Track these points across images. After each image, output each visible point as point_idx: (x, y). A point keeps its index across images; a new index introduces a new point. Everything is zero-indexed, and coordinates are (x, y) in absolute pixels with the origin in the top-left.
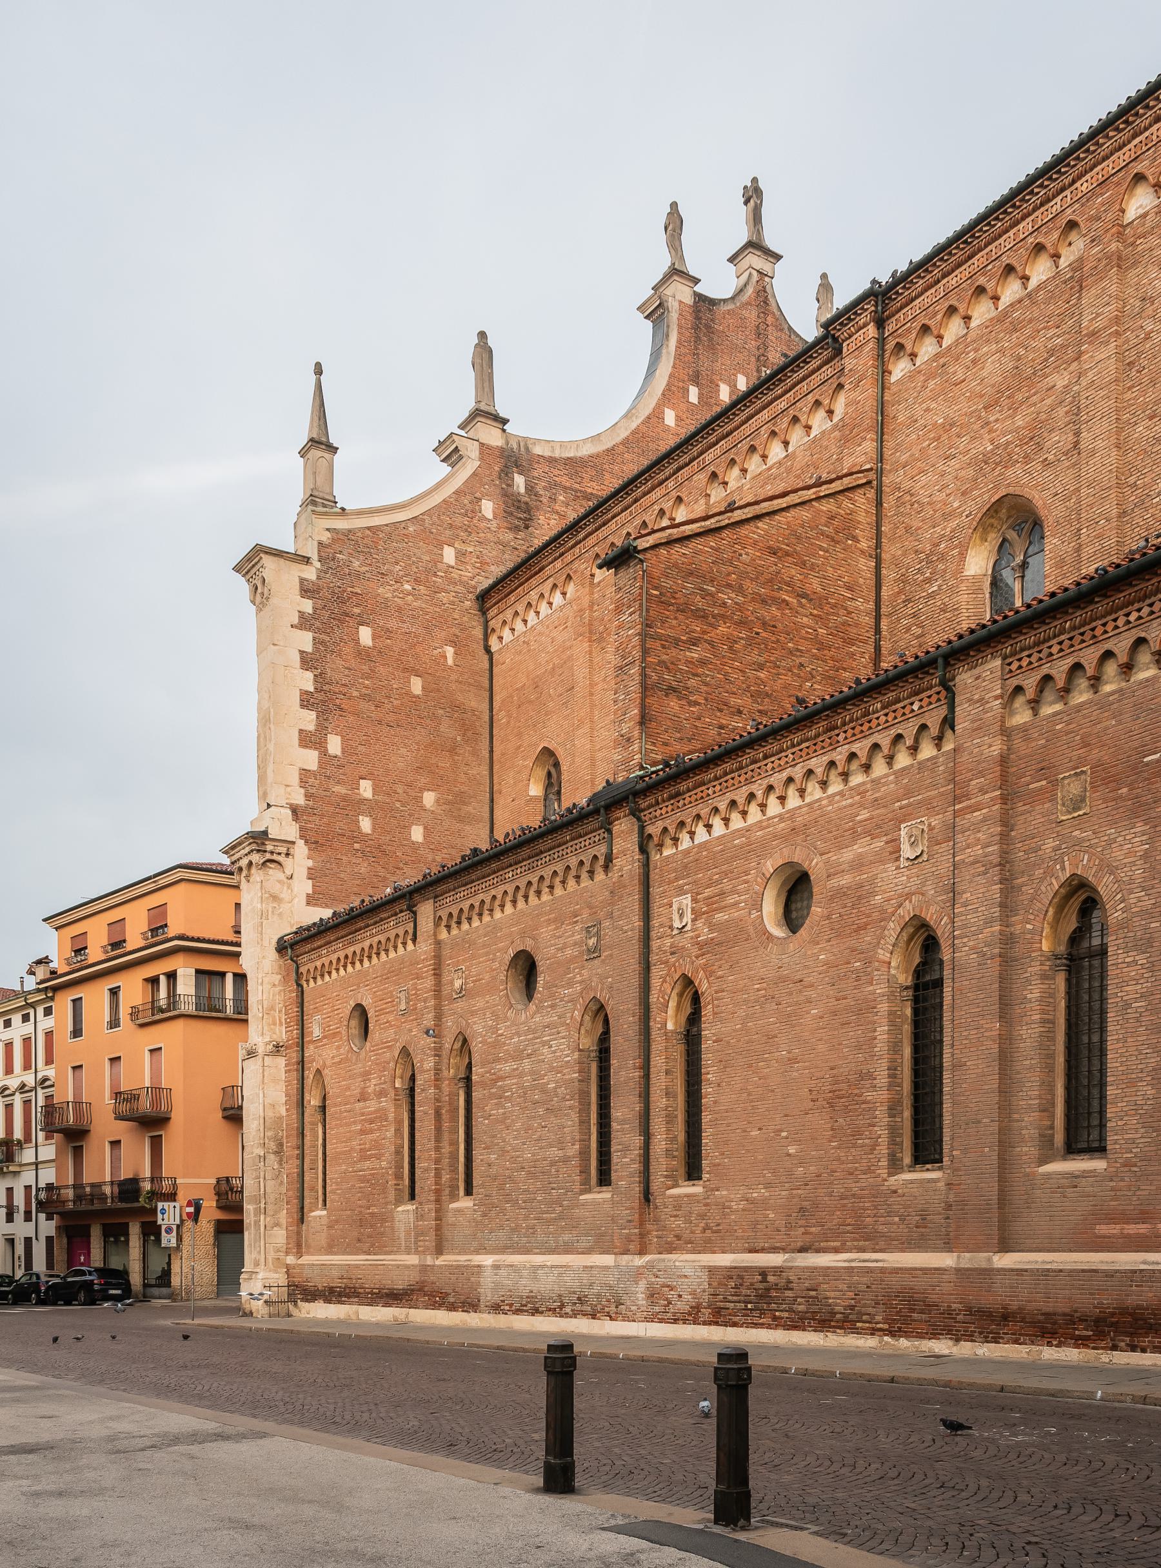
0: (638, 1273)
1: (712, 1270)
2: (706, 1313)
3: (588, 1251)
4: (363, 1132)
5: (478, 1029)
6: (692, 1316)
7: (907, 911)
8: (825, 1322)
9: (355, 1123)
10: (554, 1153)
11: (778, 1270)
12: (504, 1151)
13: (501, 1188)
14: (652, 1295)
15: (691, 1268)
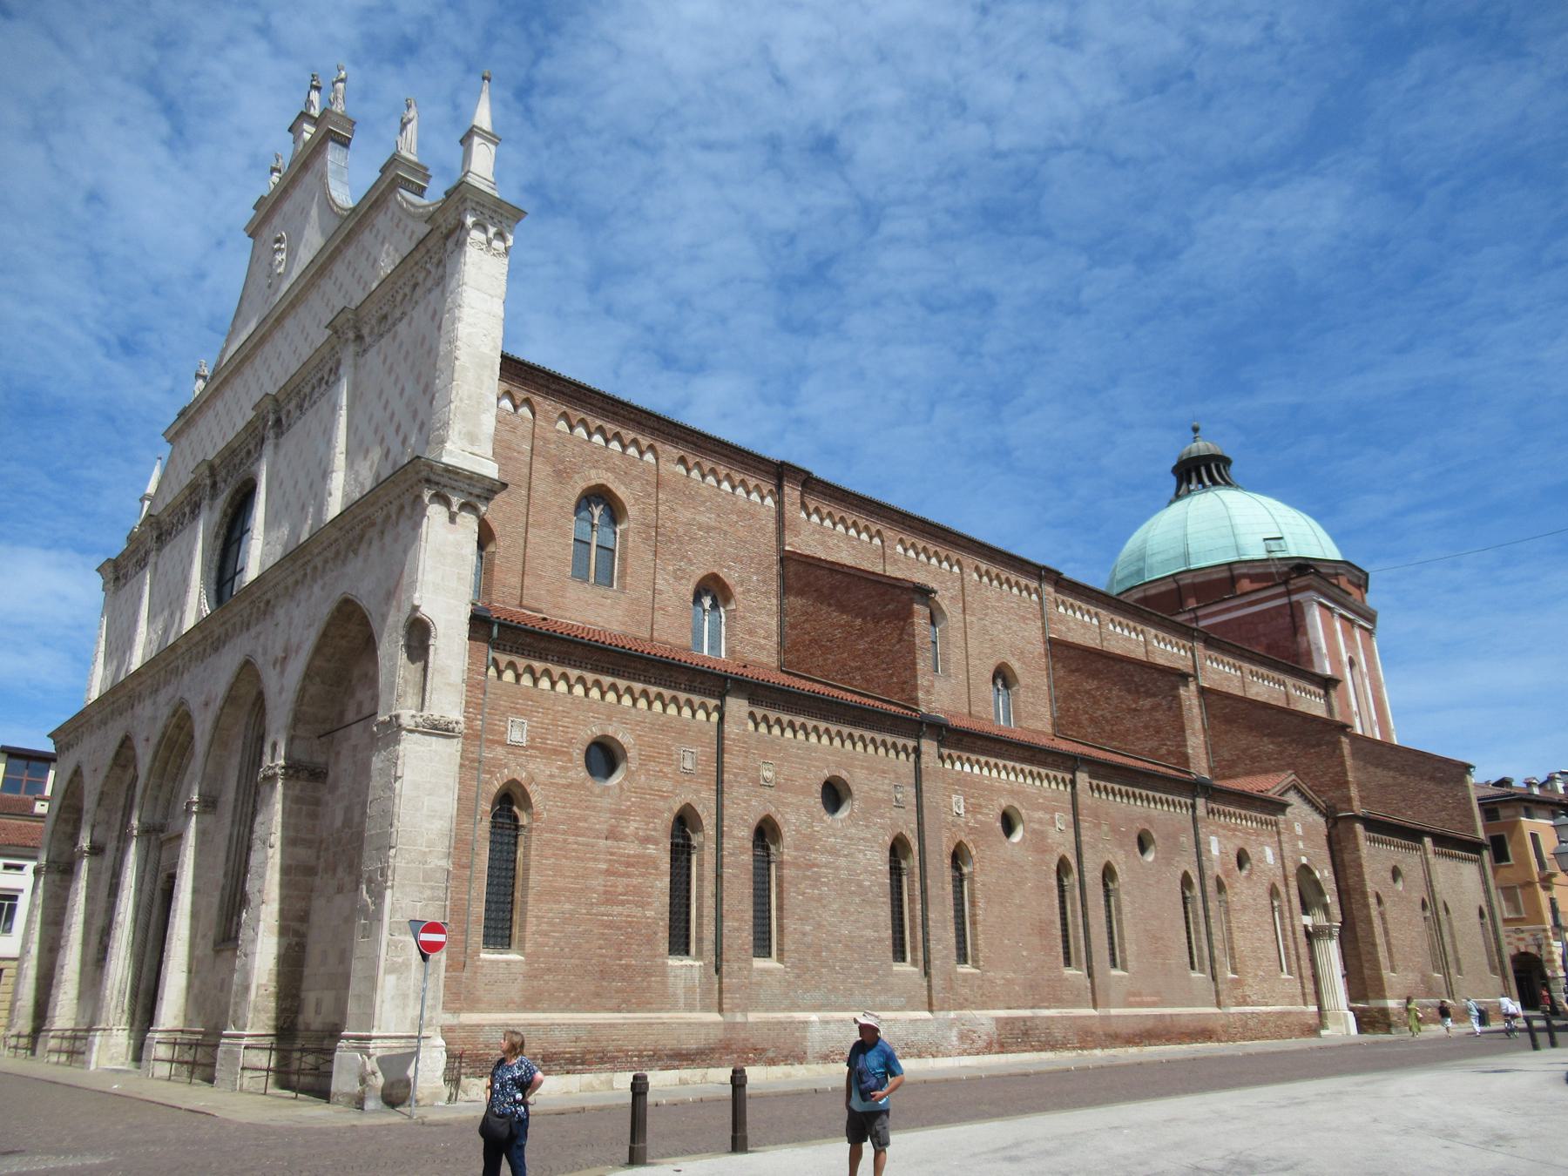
0: (951, 1024)
1: (998, 1020)
2: (996, 1047)
3: (901, 1009)
4: (608, 872)
5: (790, 824)
6: (988, 1049)
7: (1061, 851)
8: (1052, 1045)
9: (595, 860)
10: (869, 933)
11: (1032, 1018)
12: (819, 926)
13: (817, 954)
14: (963, 1037)
15: (985, 1018)
